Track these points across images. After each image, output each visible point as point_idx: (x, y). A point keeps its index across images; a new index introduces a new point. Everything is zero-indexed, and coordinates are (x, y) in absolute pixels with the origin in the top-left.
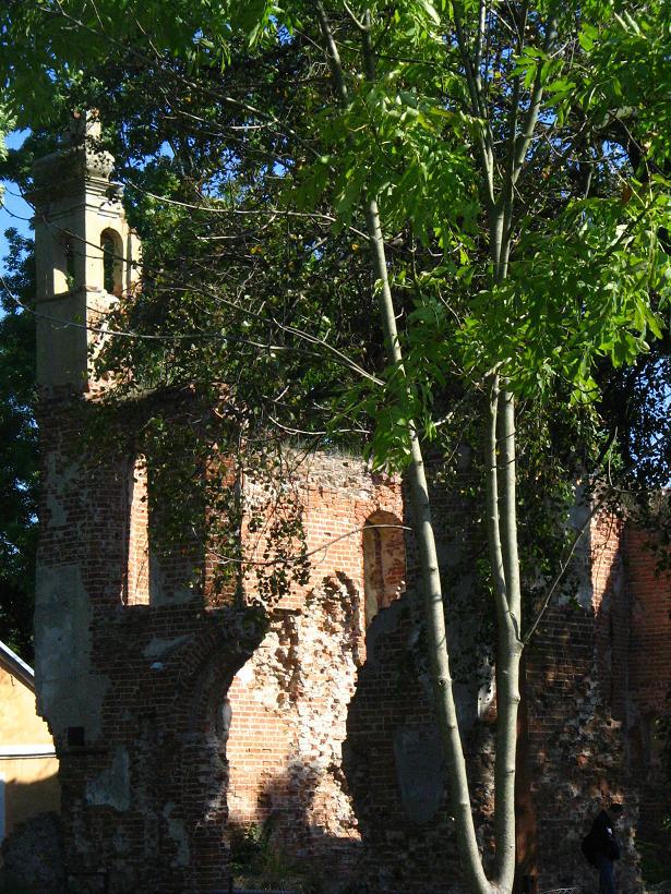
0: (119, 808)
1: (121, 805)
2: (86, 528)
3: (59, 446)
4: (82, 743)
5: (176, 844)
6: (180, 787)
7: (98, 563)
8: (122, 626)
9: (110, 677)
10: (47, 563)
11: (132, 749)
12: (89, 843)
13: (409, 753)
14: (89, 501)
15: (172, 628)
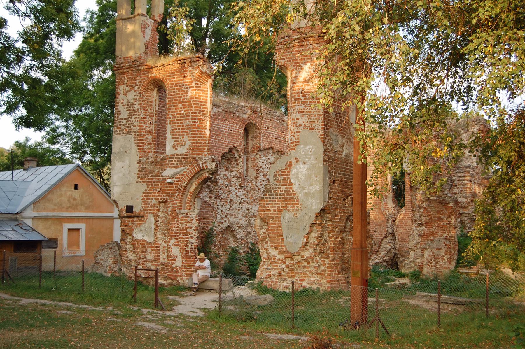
0: (149, 241)
1: (151, 240)
2: (137, 119)
3: (125, 83)
4: (132, 212)
6: (178, 233)
7: (141, 134)
8: (153, 162)
10: (118, 134)
11: (156, 216)
12: (134, 255)
14: (139, 108)
15: (177, 164)
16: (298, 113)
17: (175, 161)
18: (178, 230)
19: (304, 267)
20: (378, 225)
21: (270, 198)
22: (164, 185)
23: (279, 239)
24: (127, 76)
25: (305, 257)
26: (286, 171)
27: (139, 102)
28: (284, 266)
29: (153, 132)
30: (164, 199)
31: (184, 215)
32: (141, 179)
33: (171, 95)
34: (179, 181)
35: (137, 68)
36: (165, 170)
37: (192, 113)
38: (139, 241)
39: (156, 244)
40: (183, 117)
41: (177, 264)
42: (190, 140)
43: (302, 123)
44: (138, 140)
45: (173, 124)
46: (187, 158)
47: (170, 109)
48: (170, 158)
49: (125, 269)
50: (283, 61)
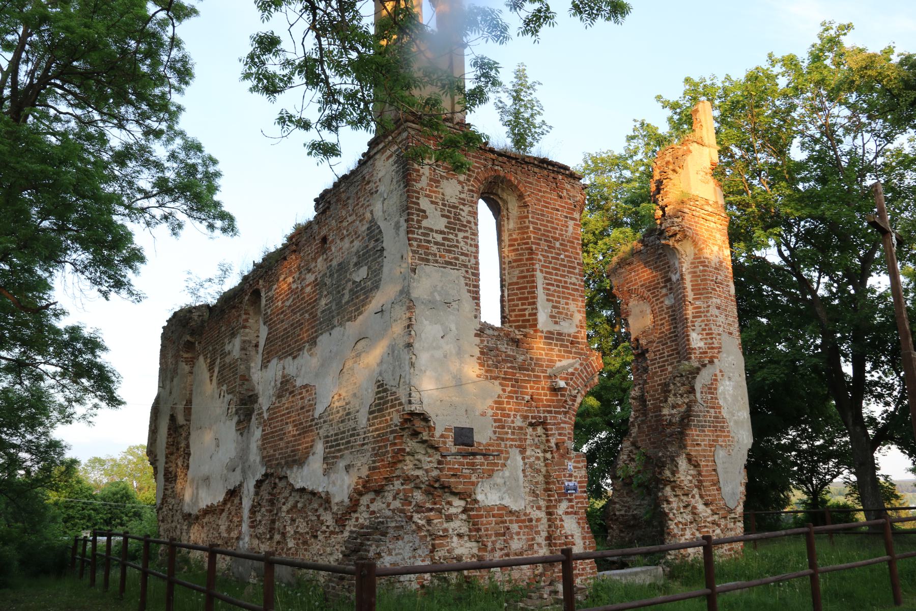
0: (514, 507)
9: (501, 384)
12: (469, 544)
15: (560, 351)
17: (556, 345)
22: (538, 389)
30: (540, 417)
40: (565, 266)
45: (547, 273)
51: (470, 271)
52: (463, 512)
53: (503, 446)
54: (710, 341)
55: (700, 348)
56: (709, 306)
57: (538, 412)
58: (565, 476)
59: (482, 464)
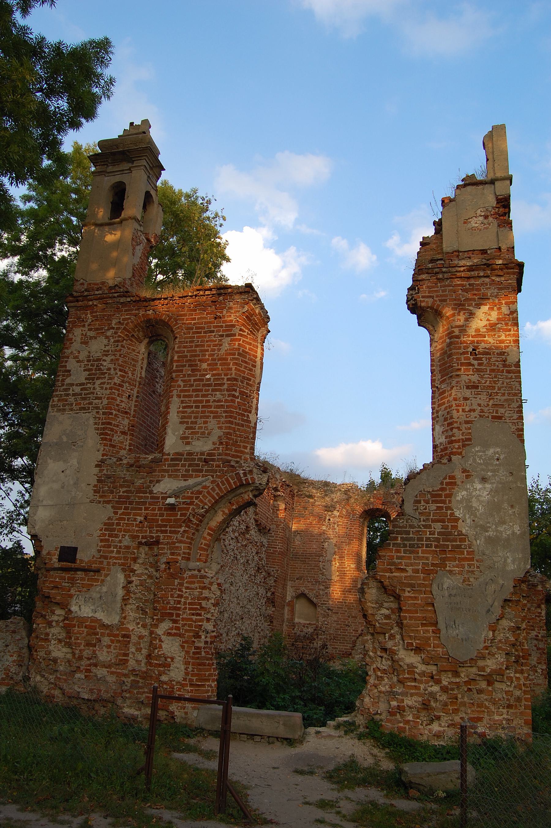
0: (106, 621)
1: (112, 619)
2: (105, 386)
4: (74, 560)
5: (169, 660)
6: (179, 609)
7: (111, 414)
8: (132, 466)
9: (112, 507)
10: (59, 410)
11: (129, 571)
12: (64, 650)
13: (450, 595)
14: (112, 366)
16: (468, 387)
18: (179, 602)
19: (480, 692)
20: (353, 617)
21: (405, 546)
22: (154, 509)
23: (428, 631)
24: (91, 313)
25: (488, 670)
26: (443, 493)
27: (113, 357)
28: (436, 688)
29: (132, 413)
30: (152, 537)
31: (196, 572)
32: (101, 497)
33: (185, 347)
34: (192, 503)
35: (118, 300)
36: (158, 481)
37: (228, 380)
38: (82, 621)
39: (123, 629)
41: (172, 674)
42: (220, 428)
43: (475, 407)
44: (103, 424)
45: (185, 396)
46: (213, 460)
47: (181, 371)
48: (172, 460)
49: (38, 678)
50: (430, 300)
51: (101, 412)
52: (64, 620)
53: (105, 563)
54: (450, 433)
55: (441, 444)
56: (452, 388)
57: (151, 532)
58: (172, 596)
59: (83, 579)
